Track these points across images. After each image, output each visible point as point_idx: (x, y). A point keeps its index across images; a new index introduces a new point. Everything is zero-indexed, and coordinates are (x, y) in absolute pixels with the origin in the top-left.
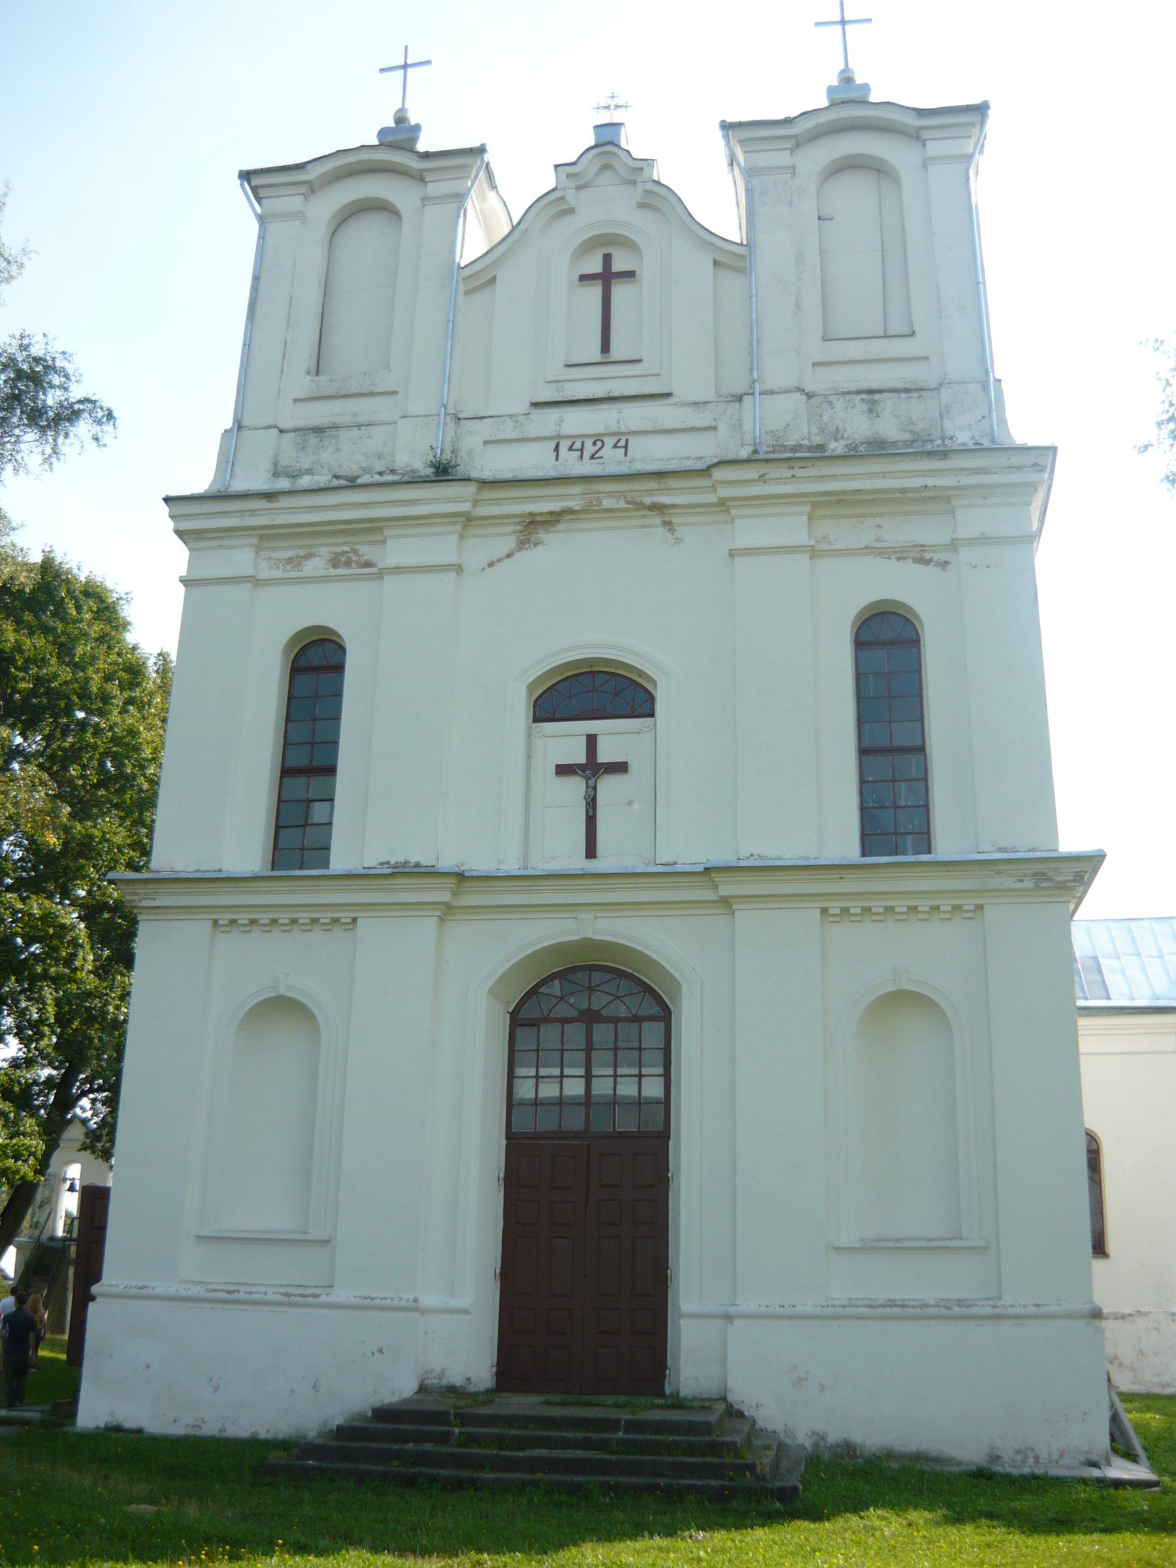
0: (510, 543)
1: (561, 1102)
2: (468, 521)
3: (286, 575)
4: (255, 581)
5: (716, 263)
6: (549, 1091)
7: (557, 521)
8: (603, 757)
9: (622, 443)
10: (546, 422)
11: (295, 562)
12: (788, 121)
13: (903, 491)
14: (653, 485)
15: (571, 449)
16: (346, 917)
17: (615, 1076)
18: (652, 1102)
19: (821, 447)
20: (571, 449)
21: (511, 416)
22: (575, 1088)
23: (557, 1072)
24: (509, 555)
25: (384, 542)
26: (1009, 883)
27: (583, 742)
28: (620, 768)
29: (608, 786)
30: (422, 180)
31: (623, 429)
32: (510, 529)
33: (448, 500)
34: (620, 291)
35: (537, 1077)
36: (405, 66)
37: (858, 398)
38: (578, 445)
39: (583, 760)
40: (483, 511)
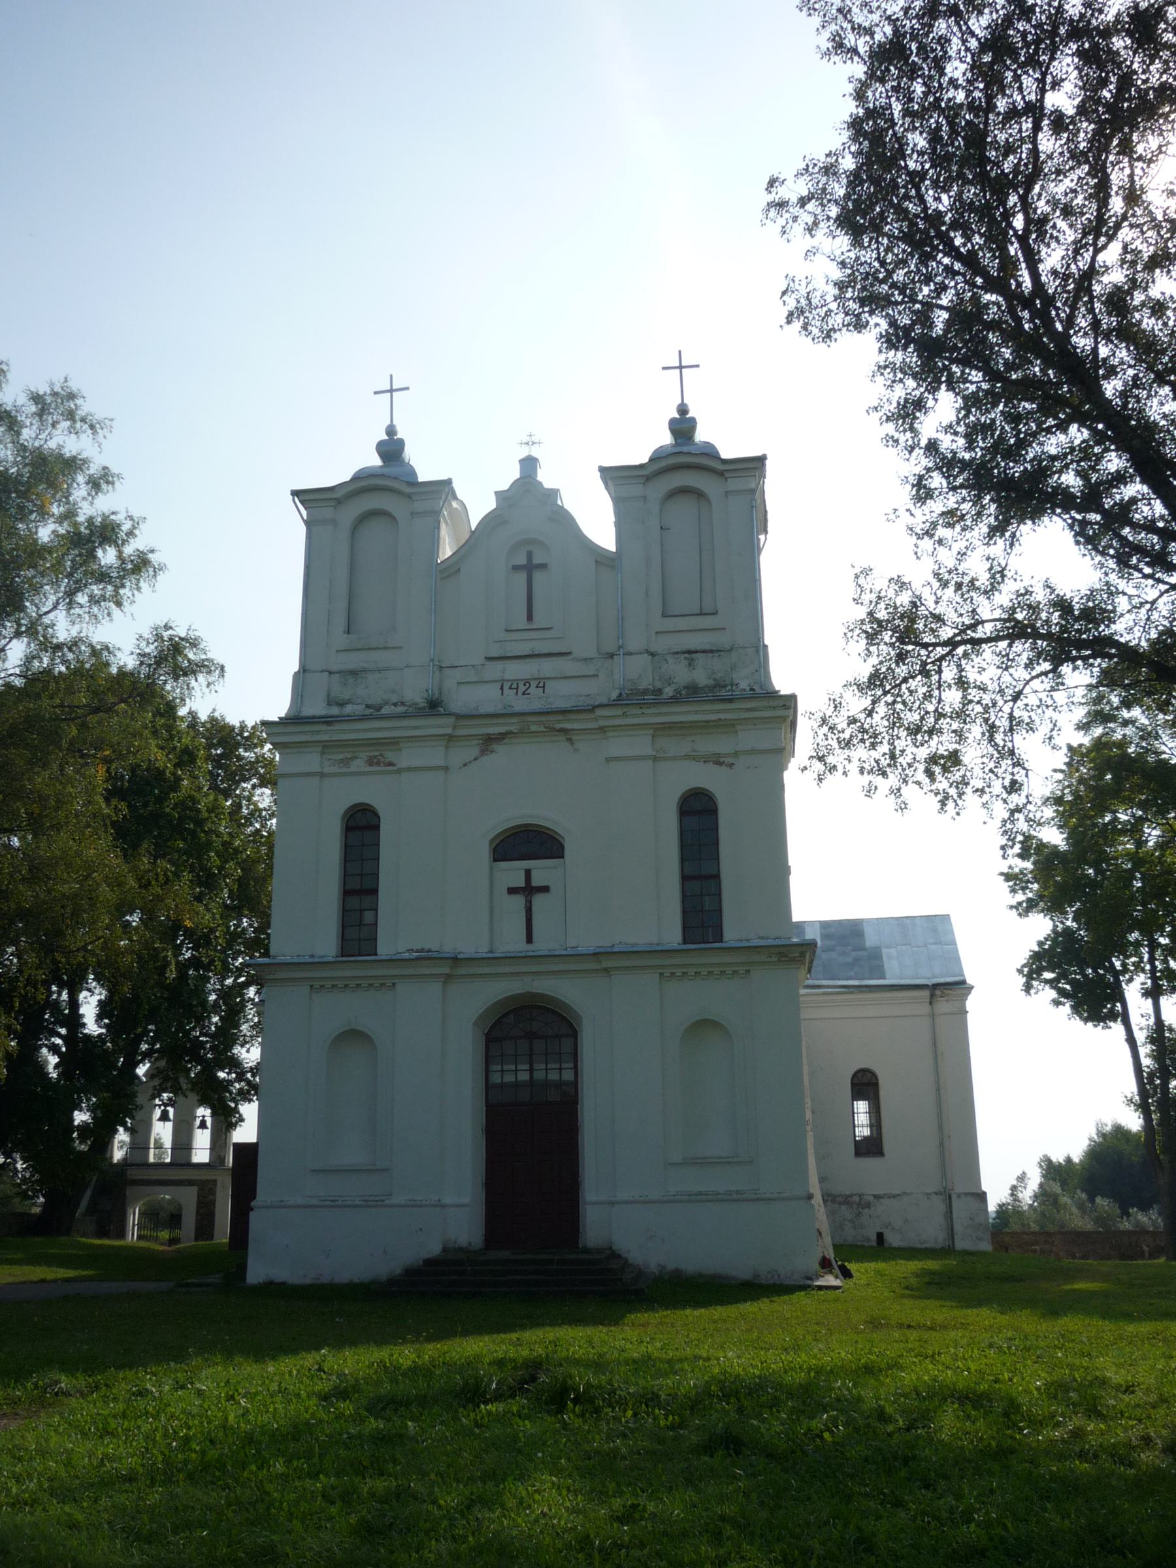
0: (475, 751)
1: (516, 1085)
2: (450, 739)
3: (340, 771)
4: (322, 775)
6: (510, 1078)
7: (504, 738)
9: (541, 685)
10: (495, 671)
11: (346, 762)
13: (707, 722)
14: (561, 717)
15: (510, 688)
16: (389, 983)
17: (546, 1069)
18: (567, 1083)
19: (659, 692)
20: (510, 688)
21: (473, 666)
22: (524, 1076)
24: (475, 759)
25: (400, 750)
26: (764, 958)
27: (523, 873)
28: (545, 889)
29: (538, 900)
30: (410, 497)
31: (542, 676)
32: (476, 742)
33: (440, 726)
34: (538, 576)
35: (502, 1071)
36: (391, 391)
37: (683, 656)
38: (514, 686)
39: (523, 885)
40: (459, 732)
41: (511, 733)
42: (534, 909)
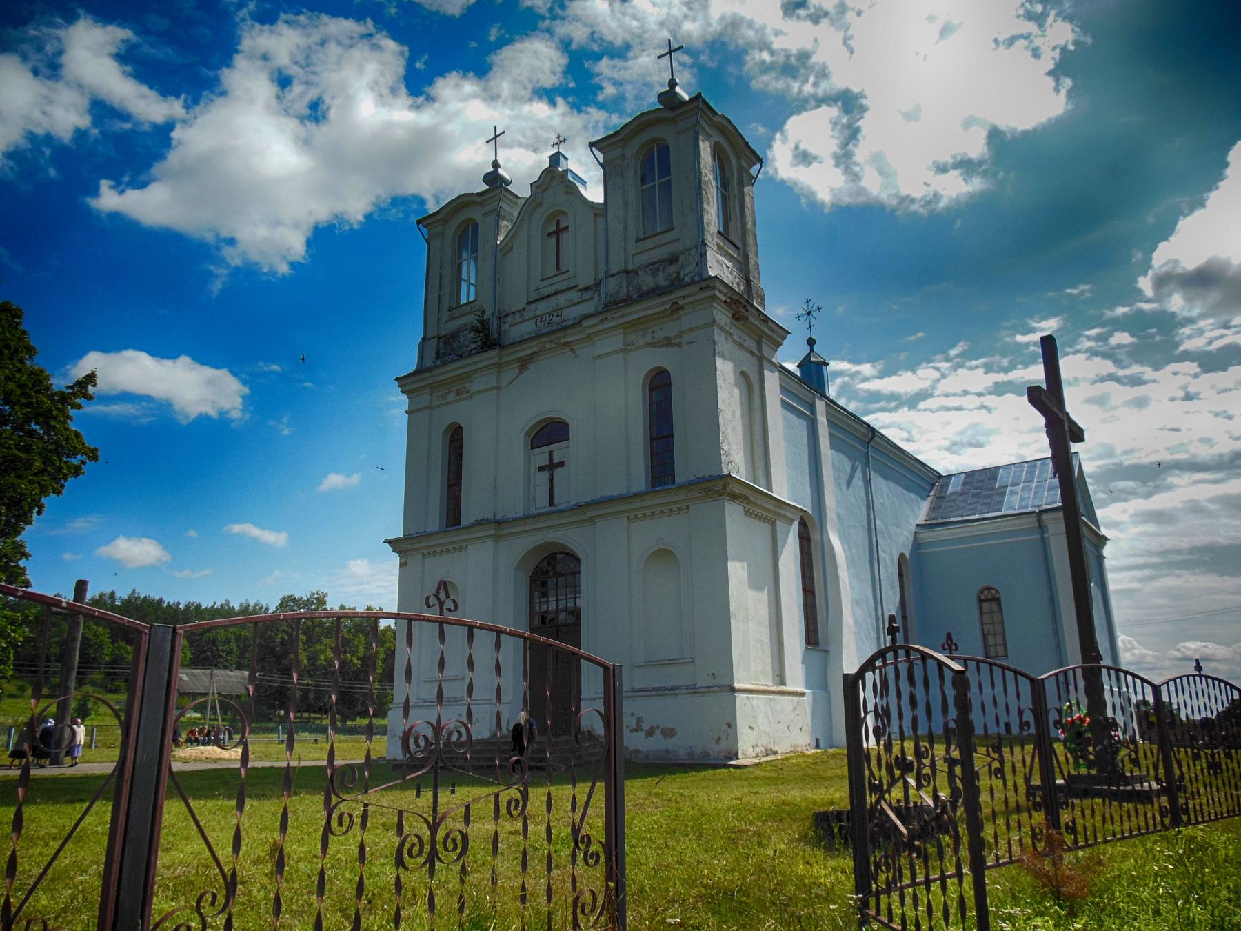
0: (517, 372)
5: (595, 214)
11: (444, 396)
13: (658, 313)
16: (463, 545)
28: (562, 464)
29: (558, 472)
34: (564, 237)
40: (504, 360)
41: (533, 354)
42: (555, 480)
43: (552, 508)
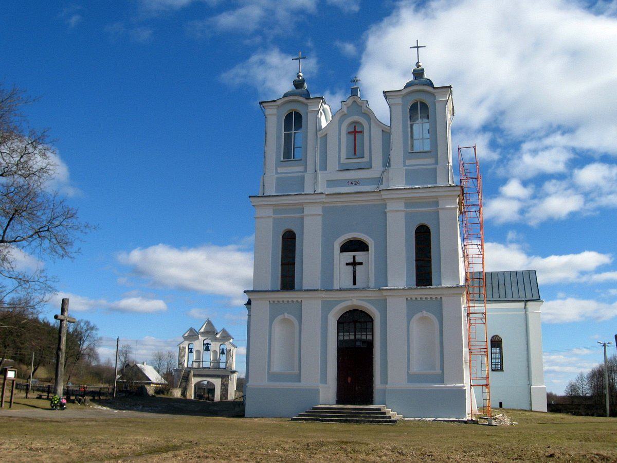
1: (350, 340)
6: (346, 338)
8: (357, 261)
12: (400, 90)
22: (352, 337)
23: (348, 334)
28: (361, 264)
29: (358, 267)
43: (355, 287)
